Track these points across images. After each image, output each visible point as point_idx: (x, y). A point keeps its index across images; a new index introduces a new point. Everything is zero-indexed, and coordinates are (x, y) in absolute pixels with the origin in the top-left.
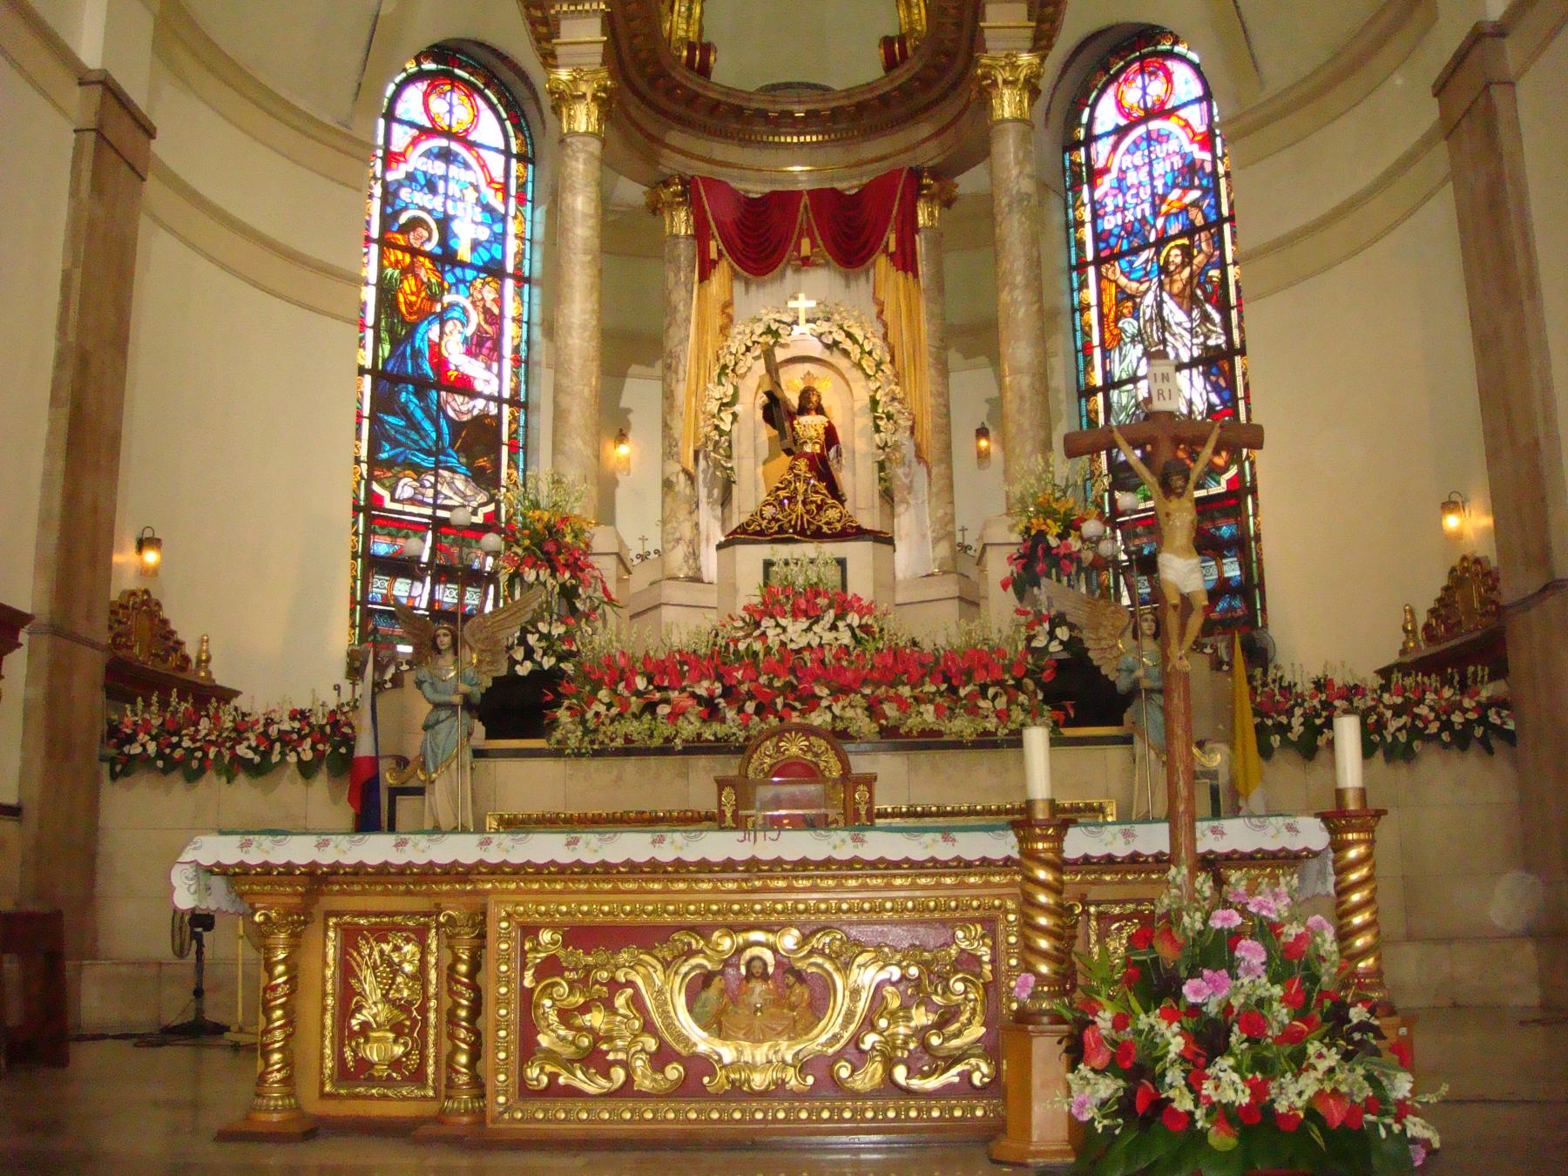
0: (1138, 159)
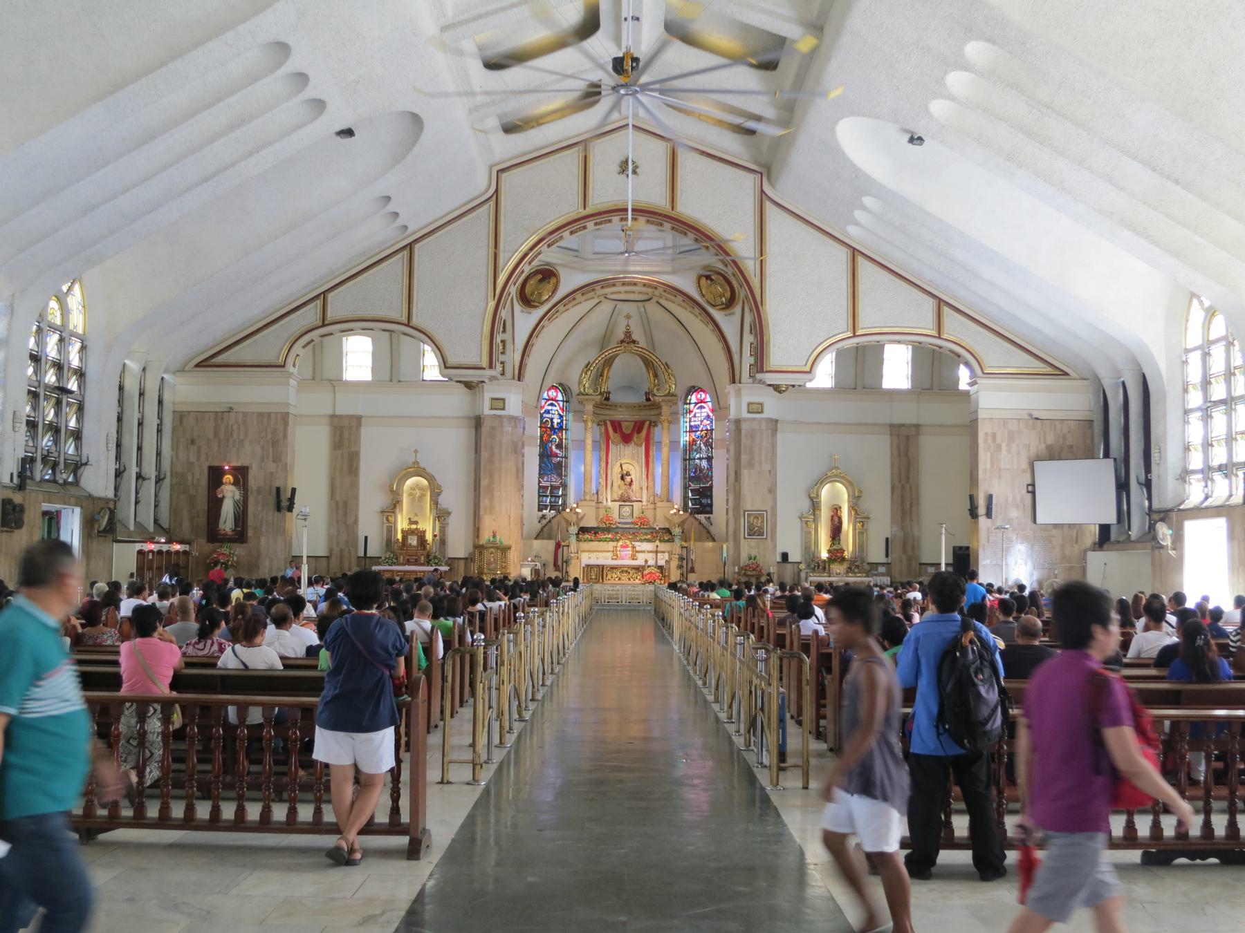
0: (698, 411)
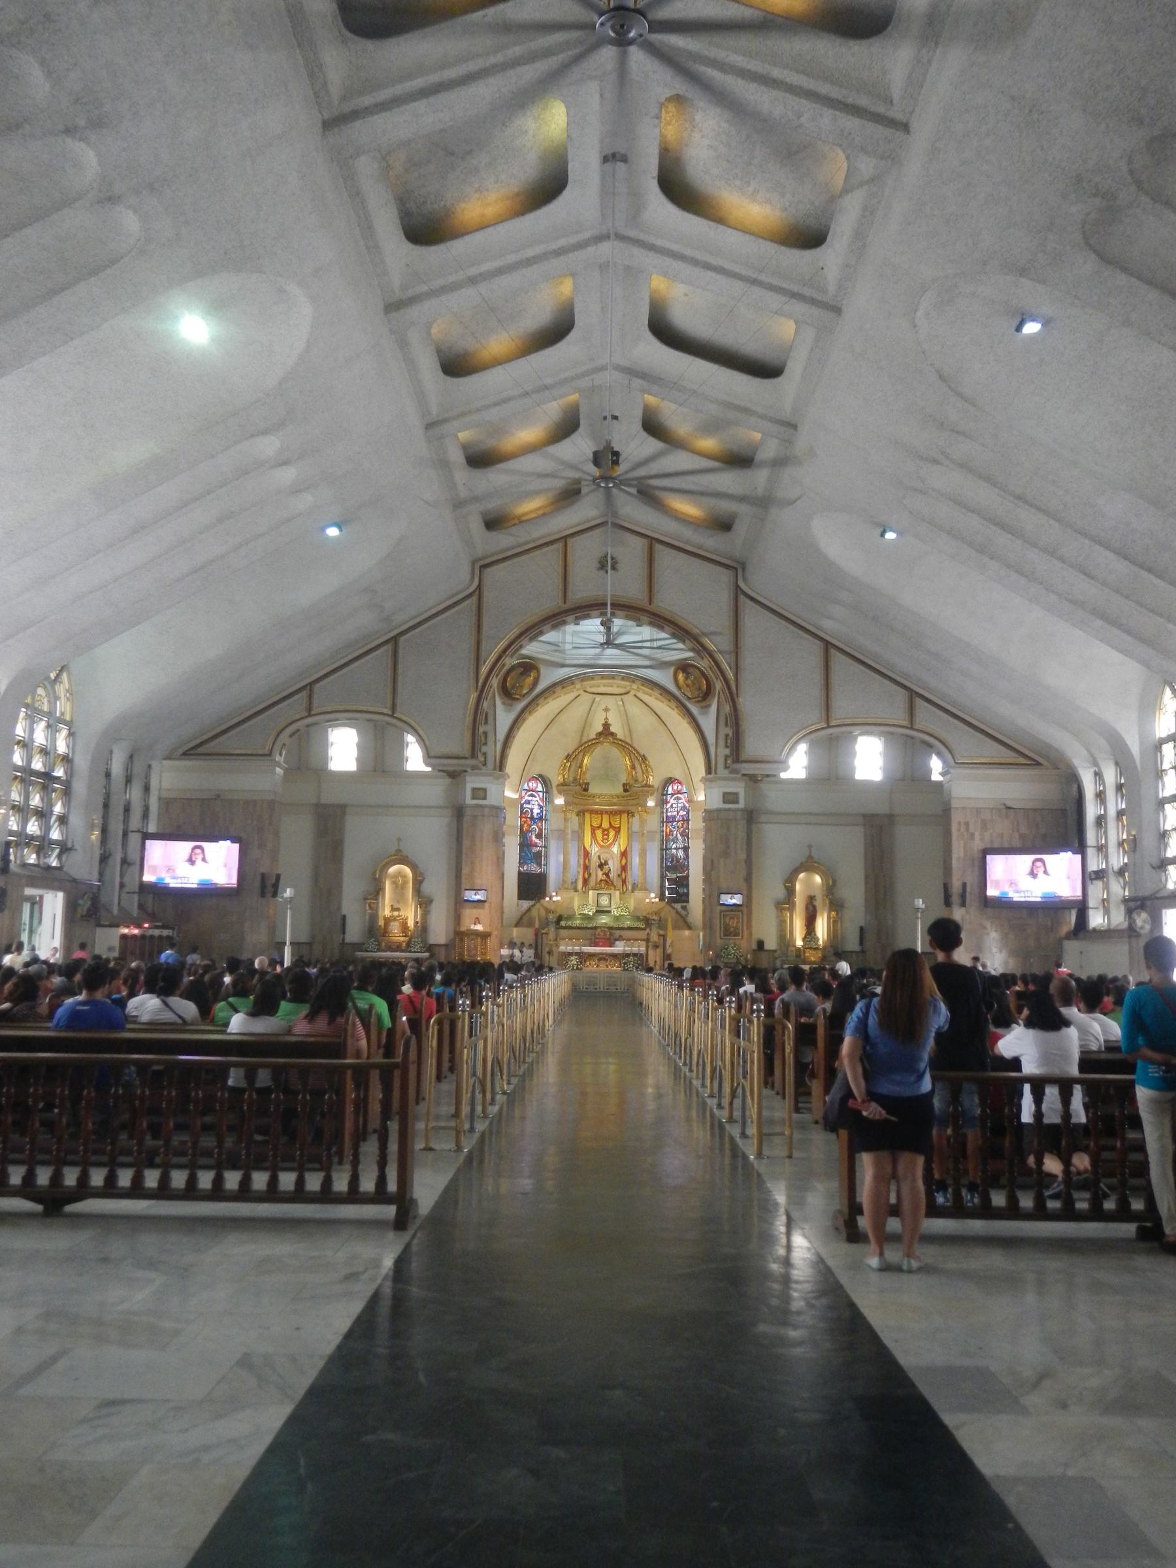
0: (675, 802)
